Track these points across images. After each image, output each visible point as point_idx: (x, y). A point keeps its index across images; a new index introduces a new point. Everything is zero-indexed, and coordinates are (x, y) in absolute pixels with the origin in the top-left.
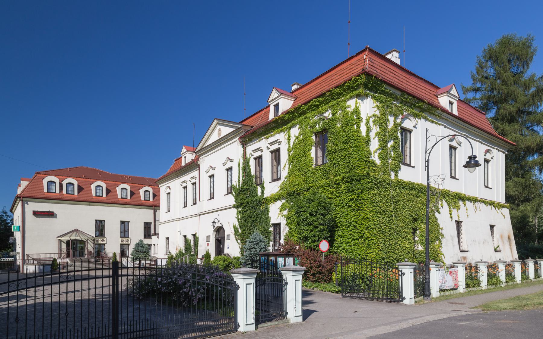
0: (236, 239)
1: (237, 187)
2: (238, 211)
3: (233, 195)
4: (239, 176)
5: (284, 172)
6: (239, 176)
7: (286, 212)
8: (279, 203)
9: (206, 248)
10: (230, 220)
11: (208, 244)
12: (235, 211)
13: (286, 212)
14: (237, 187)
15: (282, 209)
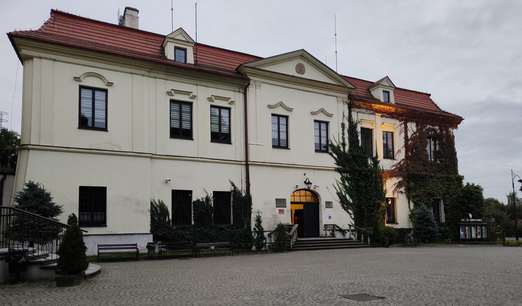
0: (344, 208)
1: (342, 149)
2: (342, 175)
3: (333, 156)
4: (343, 139)
5: (400, 156)
6: (343, 139)
7: (402, 189)
8: (395, 180)
9: (274, 216)
10: (329, 185)
11: (281, 212)
12: (338, 176)
13: (402, 189)
14: (342, 149)
15: (399, 185)
